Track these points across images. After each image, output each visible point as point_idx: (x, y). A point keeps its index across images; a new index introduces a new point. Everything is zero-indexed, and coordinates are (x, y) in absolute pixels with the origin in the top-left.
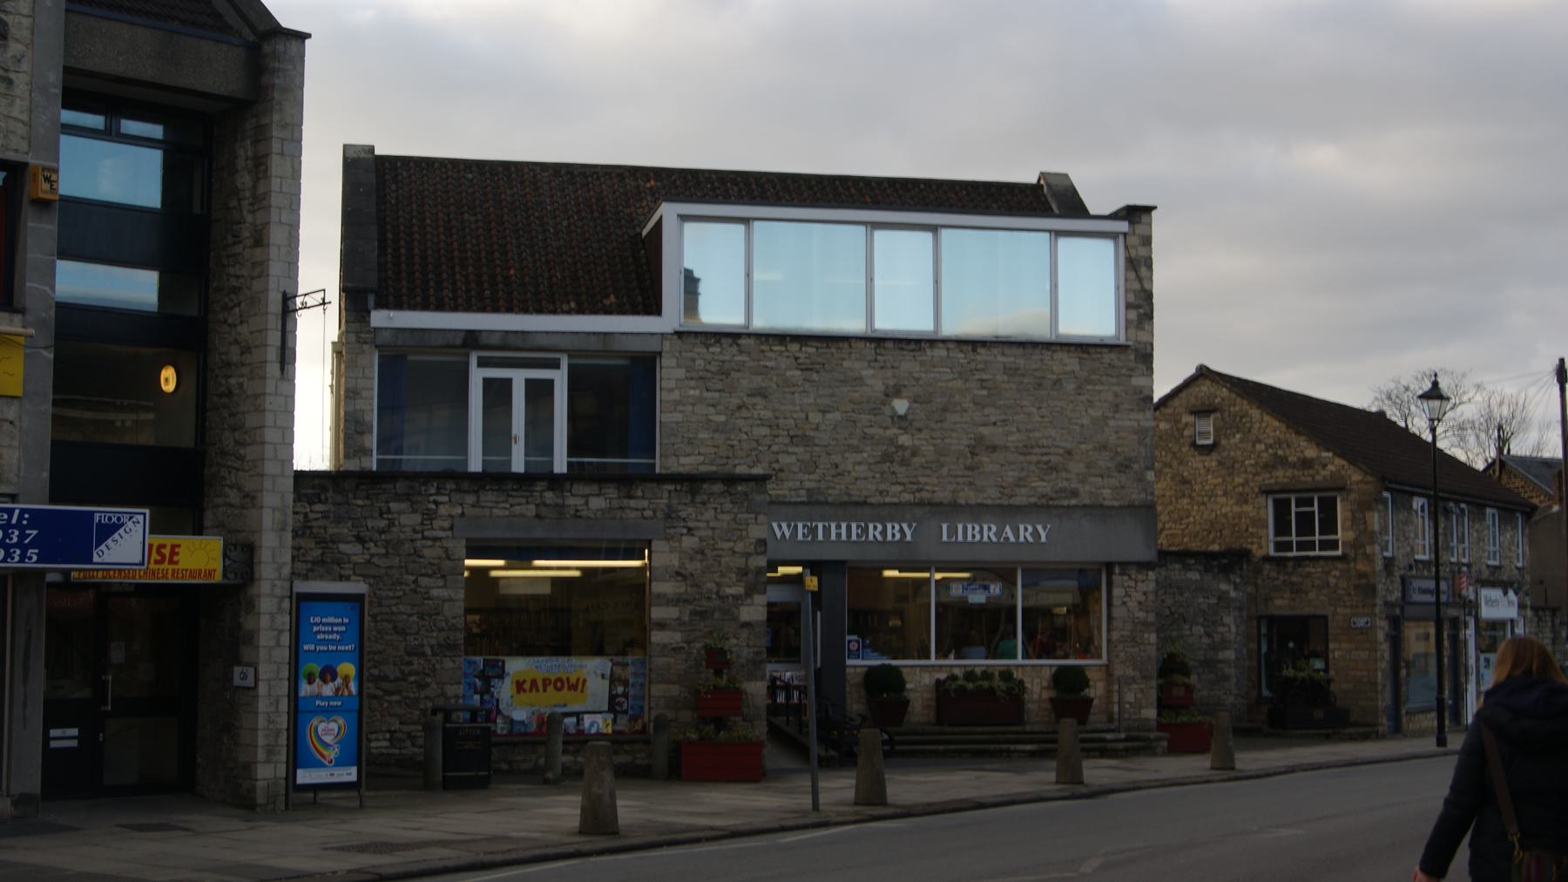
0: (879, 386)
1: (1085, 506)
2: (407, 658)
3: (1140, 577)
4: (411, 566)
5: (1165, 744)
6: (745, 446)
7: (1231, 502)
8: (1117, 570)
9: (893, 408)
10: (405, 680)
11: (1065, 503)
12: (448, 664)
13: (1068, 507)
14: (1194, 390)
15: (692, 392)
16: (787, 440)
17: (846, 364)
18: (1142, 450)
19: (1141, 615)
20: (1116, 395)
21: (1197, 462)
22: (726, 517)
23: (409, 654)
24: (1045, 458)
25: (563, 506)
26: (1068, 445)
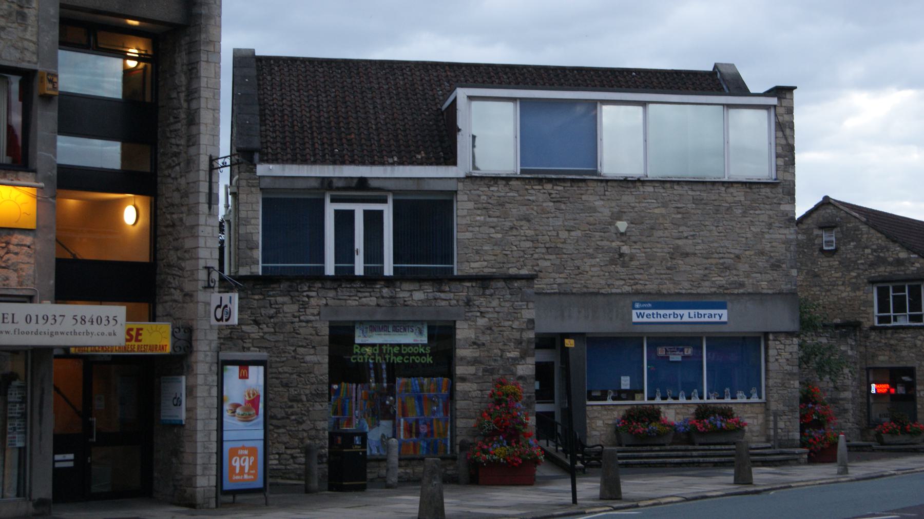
0: (607, 212)
1: (749, 294)
2: (290, 404)
3: (788, 342)
4: (292, 340)
5: (806, 456)
6: (515, 254)
7: (849, 289)
8: (771, 337)
9: (617, 228)
10: (288, 418)
11: (736, 291)
12: (318, 407)
13: (738, 294)
14: (822, 212)
15: (478, 218)
16: (544, 250)
17: (584, 197)
18: (788, 254)
19: (788, 368)
20: (770, 217)
21: (824, 262)
22: (508, 304)
23: (291, 401)
24: (721, 261)
25: (395, 298)
26: (737, 252)
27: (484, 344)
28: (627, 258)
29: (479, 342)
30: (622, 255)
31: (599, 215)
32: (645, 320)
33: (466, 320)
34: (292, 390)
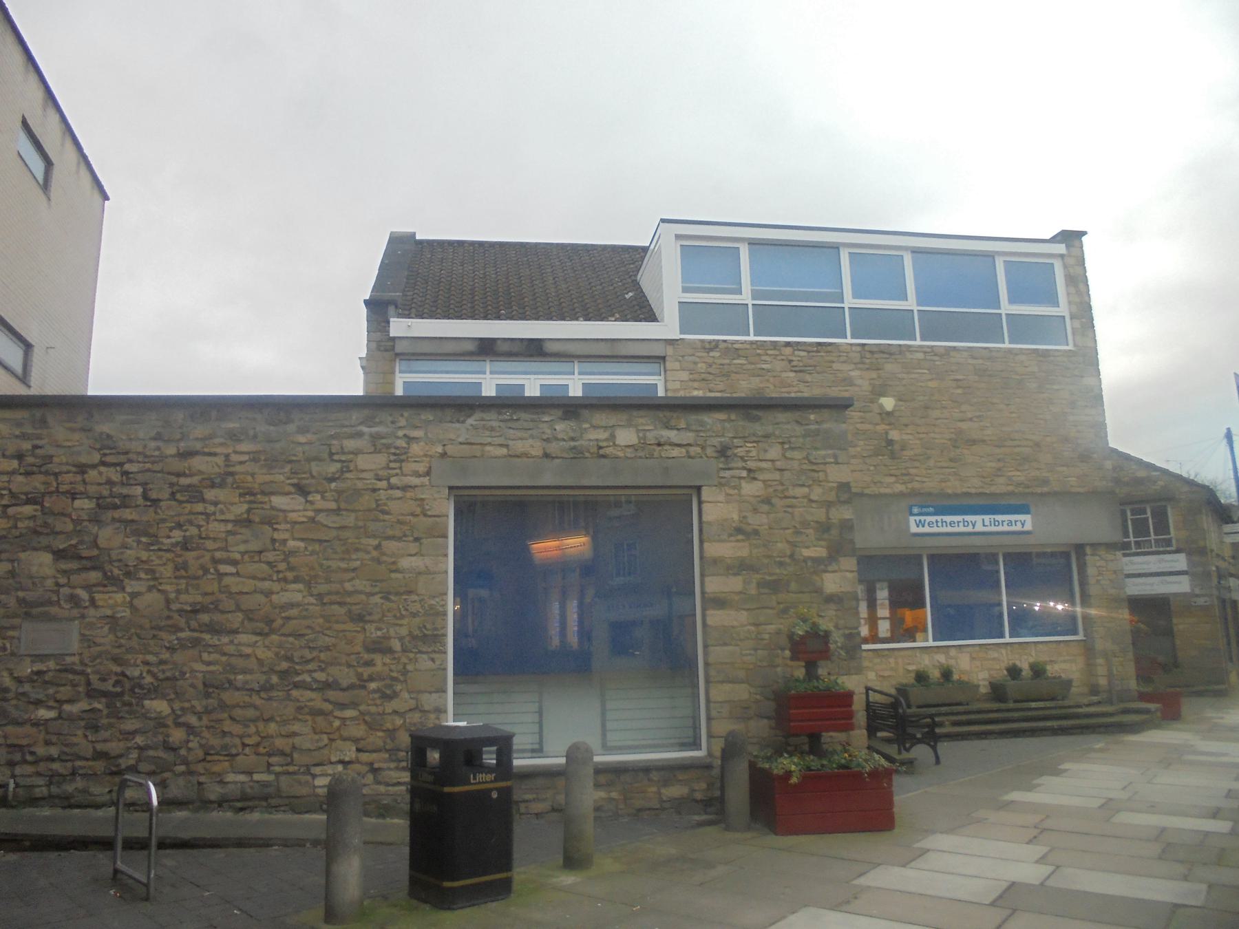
0: (866, 386)
1: (1056, 494)
2: (366, 656)
3: (1110, 557)
4: (372, 526)
8: (1088, 550)
9: (881, 406)
10: (364, 687)
11: (1039, 490)
13: (1042, 495)
17: (835, 366)
22: (797, 455)
23: (368, 650)
27: (756, 532)
28: (897, 447)
29: (749, 529)
30: (890, 442)
31: (856, 389)
32: (927, 529)
33: (721, 485)
34: (370, 628)
